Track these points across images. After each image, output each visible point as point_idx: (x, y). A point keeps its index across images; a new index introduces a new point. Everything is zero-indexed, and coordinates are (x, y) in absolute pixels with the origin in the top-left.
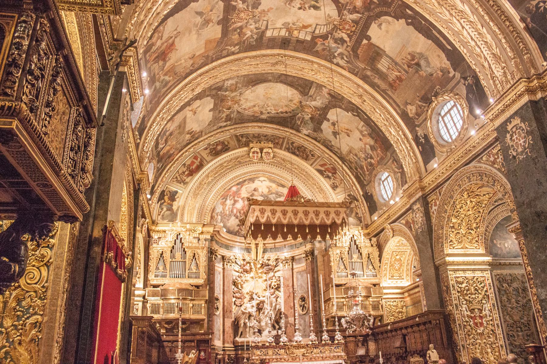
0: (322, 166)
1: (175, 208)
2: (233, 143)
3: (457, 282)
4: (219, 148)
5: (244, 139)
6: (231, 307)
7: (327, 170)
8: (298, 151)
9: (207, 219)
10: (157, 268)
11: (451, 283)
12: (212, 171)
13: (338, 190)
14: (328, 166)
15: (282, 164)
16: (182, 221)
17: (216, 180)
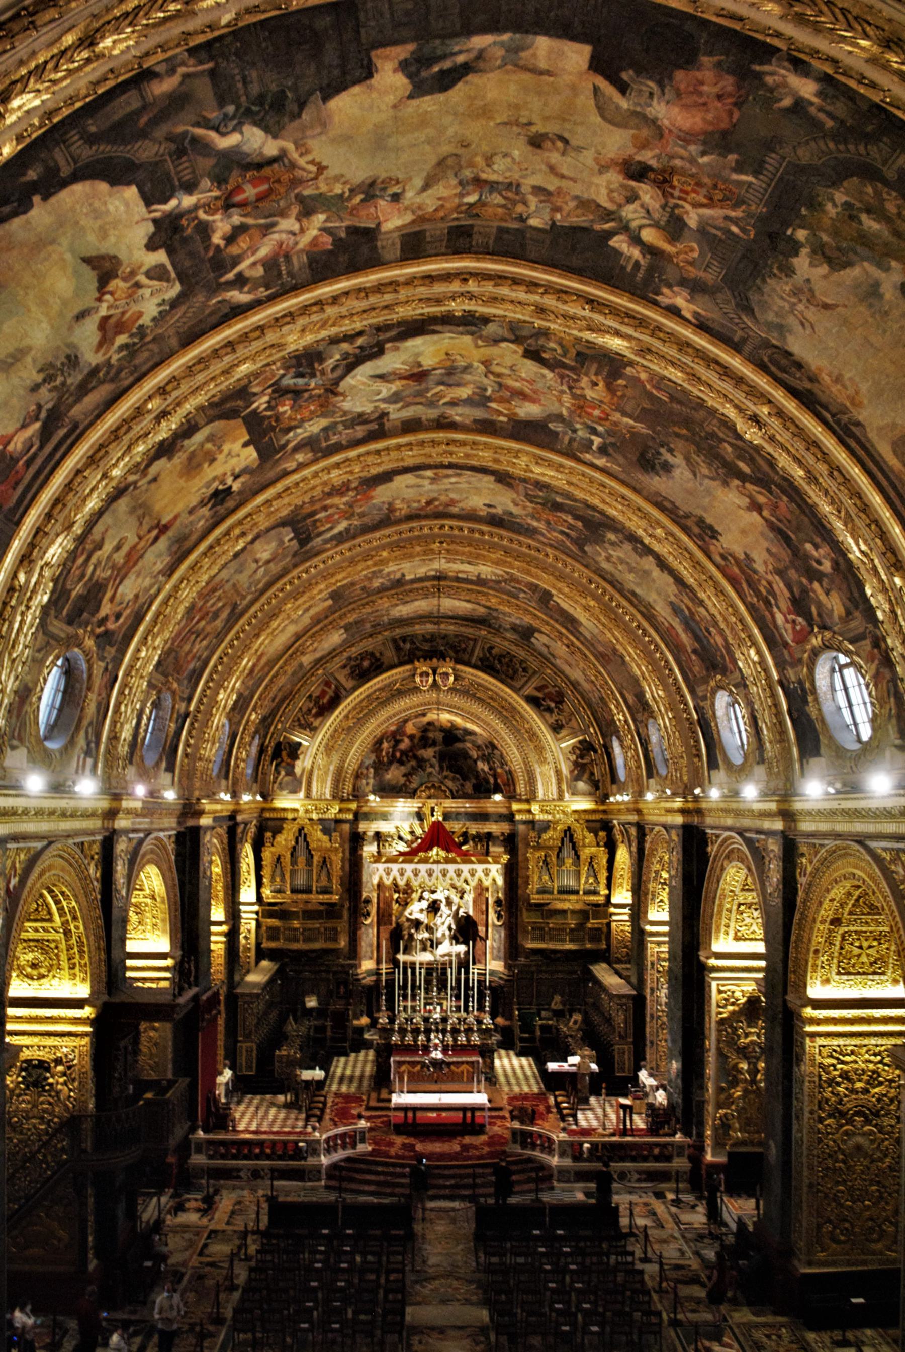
0: (538, 689)
1: (298, 770)
2: (390, 655)
3: (659, 959)
4: (366, 664)
5: (408, 646)
6: (390, 907)
7: (549, 696)
8: (500, 662)
9: (348, 787)
10: (273, 880)
11: (649, 959)
12: (354, 708)
13: (564, 733)
14: (550, 689)
15: (468, 692)
16: (308, 796)
17: (360, 722)
